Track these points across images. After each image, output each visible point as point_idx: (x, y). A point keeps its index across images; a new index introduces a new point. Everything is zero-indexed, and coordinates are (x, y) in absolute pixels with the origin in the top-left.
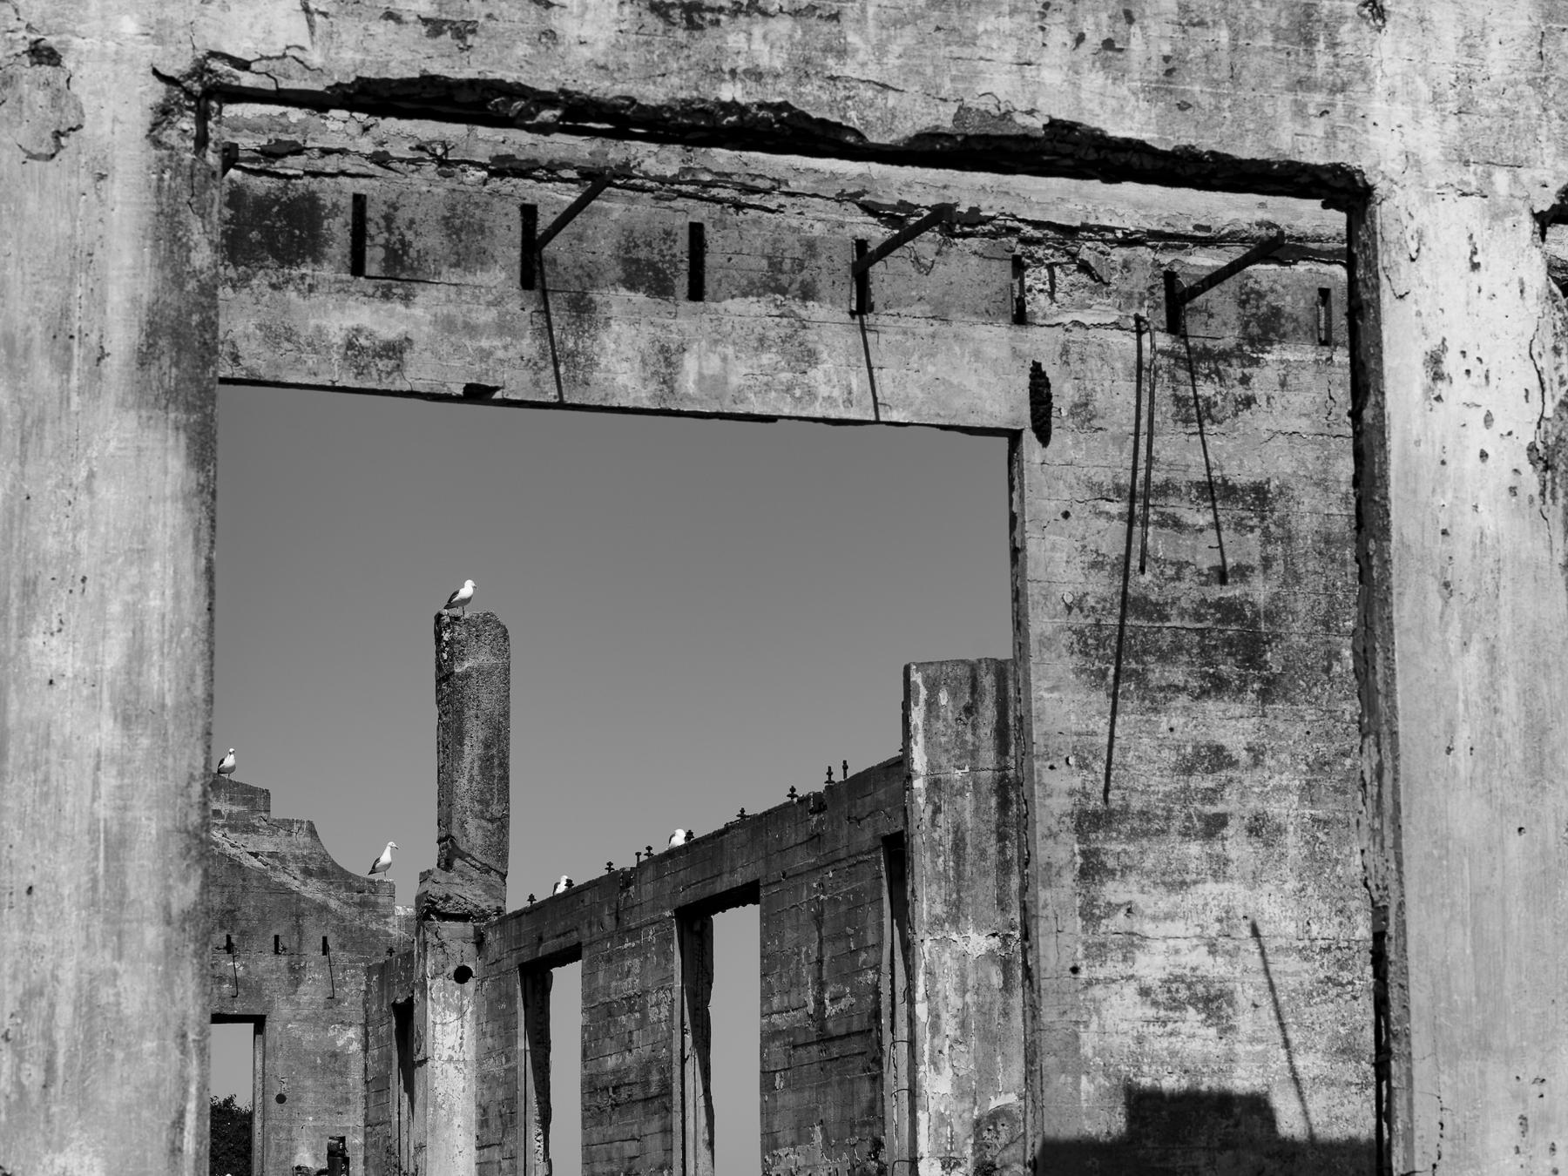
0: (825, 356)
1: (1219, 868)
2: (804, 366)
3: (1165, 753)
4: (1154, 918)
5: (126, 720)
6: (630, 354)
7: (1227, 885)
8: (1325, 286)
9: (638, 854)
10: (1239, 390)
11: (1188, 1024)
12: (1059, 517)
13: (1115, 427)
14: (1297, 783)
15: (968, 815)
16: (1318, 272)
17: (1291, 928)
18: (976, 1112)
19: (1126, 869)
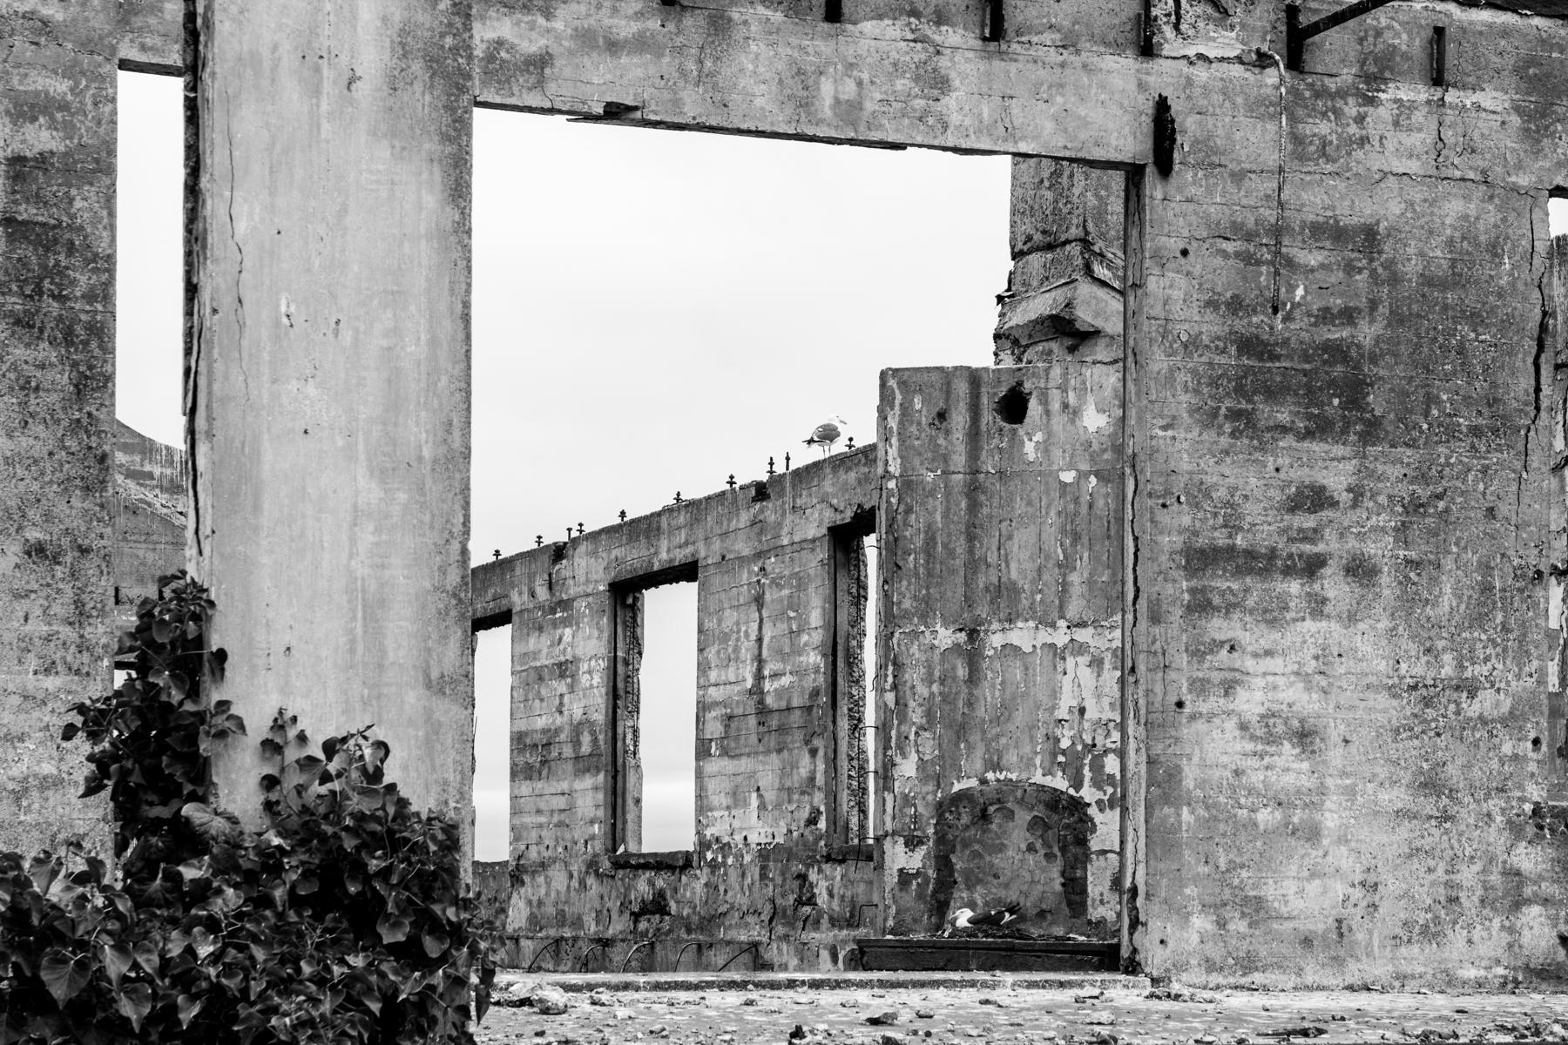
0: (957, 83)
1: (1318, 606)
2: (936, 92)
3: (1271, 493)
4: (1256, 655)
5: (382, 474)
6: (768, 76)
7: (1324, 624)
8: (1440, 25)
9: (569, 530)
10: (1353, 129)
11: (1283, 757)
12: (1178, 254)
13: (1234, 164)
14: (1393, 524)
15: (938, 517)
16: (1434, 10)
17: (1382, 666)
18: (939, 795)
19: (1229, 608)
